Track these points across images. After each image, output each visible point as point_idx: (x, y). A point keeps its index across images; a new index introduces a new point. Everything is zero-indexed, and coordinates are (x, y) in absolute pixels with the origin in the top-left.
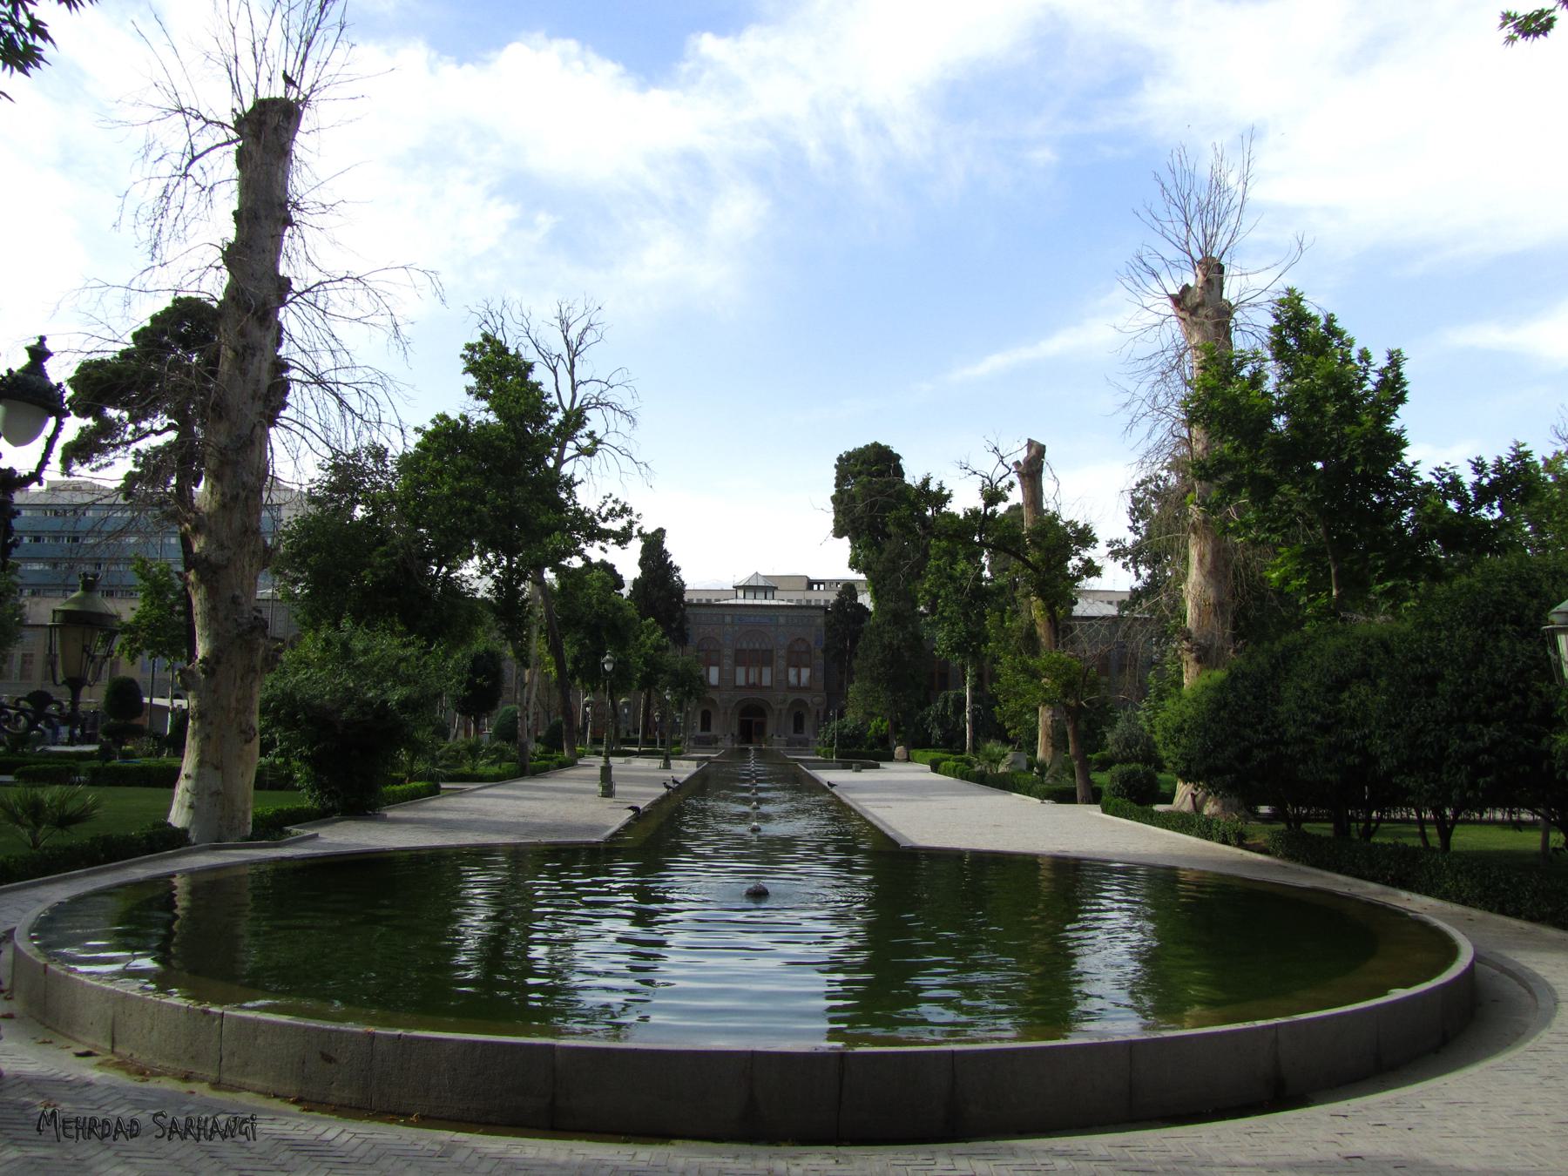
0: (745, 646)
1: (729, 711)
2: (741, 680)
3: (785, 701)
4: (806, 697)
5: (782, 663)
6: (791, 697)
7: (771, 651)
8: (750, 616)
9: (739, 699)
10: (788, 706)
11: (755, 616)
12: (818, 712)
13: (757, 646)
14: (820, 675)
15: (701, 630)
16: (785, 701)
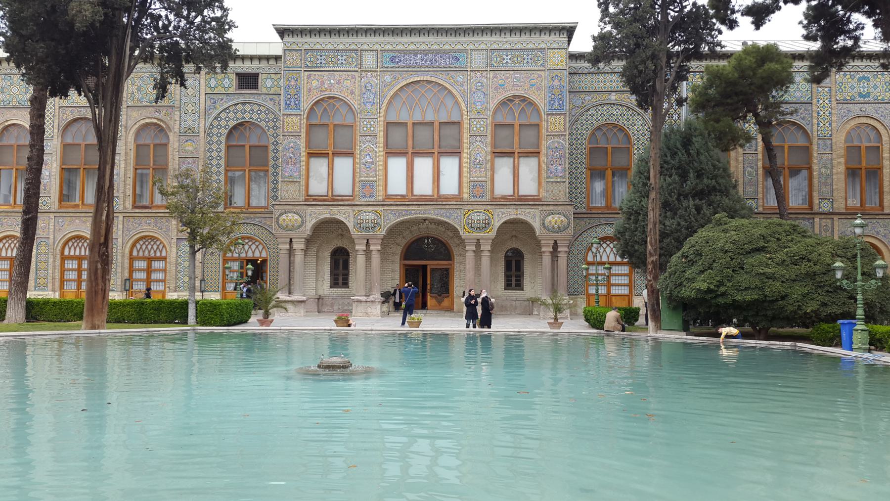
0: (404, 117)
1: (375, 247)
2: (397, 185)
3: (487, 224)
4: (532, 217)
5: (483, 149)
6: (500, 217)
7: (458, 124)
8: (415, 52)
9: (394, 220)
10: (493, 234)
11: (425, 52)
12: (555, 246)
13: (429, 118)
14: (560, 169)
15: (315, 83)
16: (487, 224)
